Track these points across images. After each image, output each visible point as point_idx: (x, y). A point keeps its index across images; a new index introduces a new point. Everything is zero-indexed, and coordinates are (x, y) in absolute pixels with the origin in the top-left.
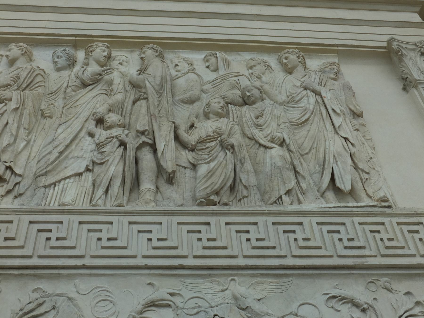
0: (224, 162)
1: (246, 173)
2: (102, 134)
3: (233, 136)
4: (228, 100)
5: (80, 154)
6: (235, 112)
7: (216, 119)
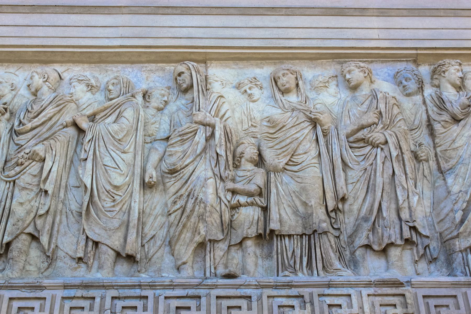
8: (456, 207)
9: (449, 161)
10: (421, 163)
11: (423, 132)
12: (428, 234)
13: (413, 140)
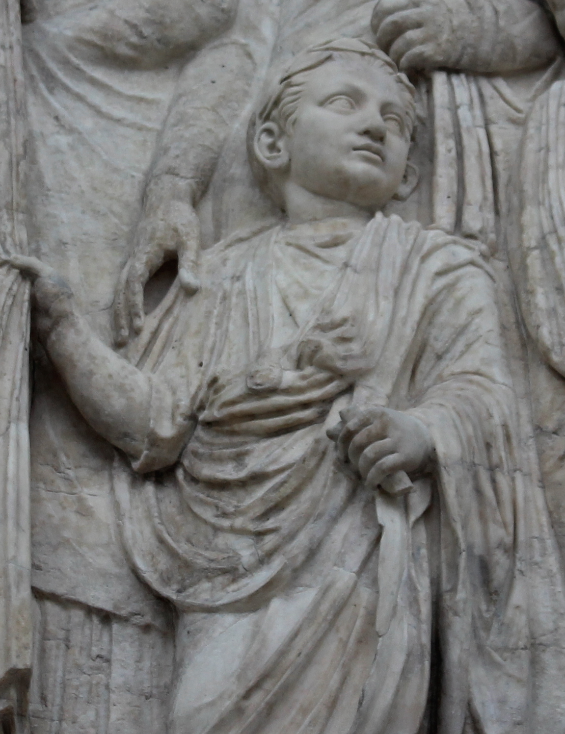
0: (365, 594)
1: (518, 666)
3: (450, 366)
4: (428, 49)
6: (474, 141)
7: (324, 231)
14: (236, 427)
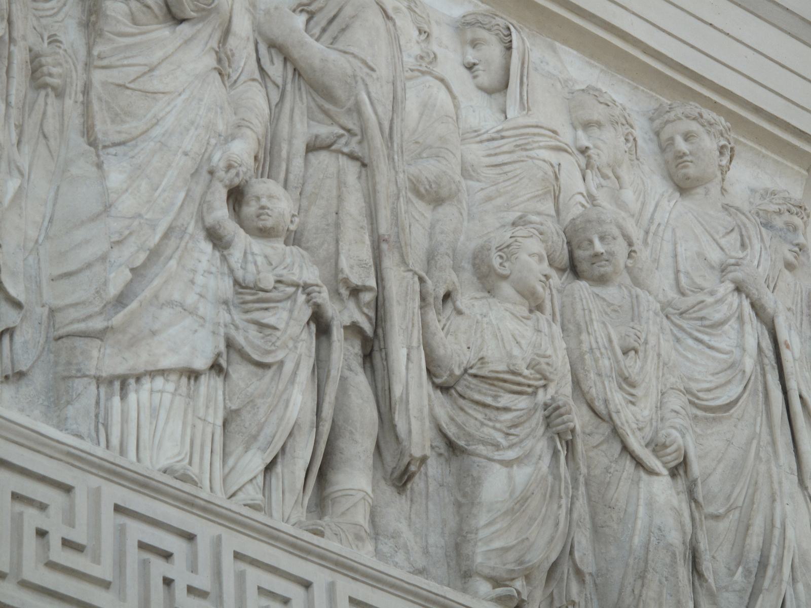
2: (255, 256)
5: (191, 299)
8: (114, 254)
9: (123, 122)
10: (43, 93)
11: (65, 9)
12: (21, 298)
13: (39, 18)
14: (496, 383)
